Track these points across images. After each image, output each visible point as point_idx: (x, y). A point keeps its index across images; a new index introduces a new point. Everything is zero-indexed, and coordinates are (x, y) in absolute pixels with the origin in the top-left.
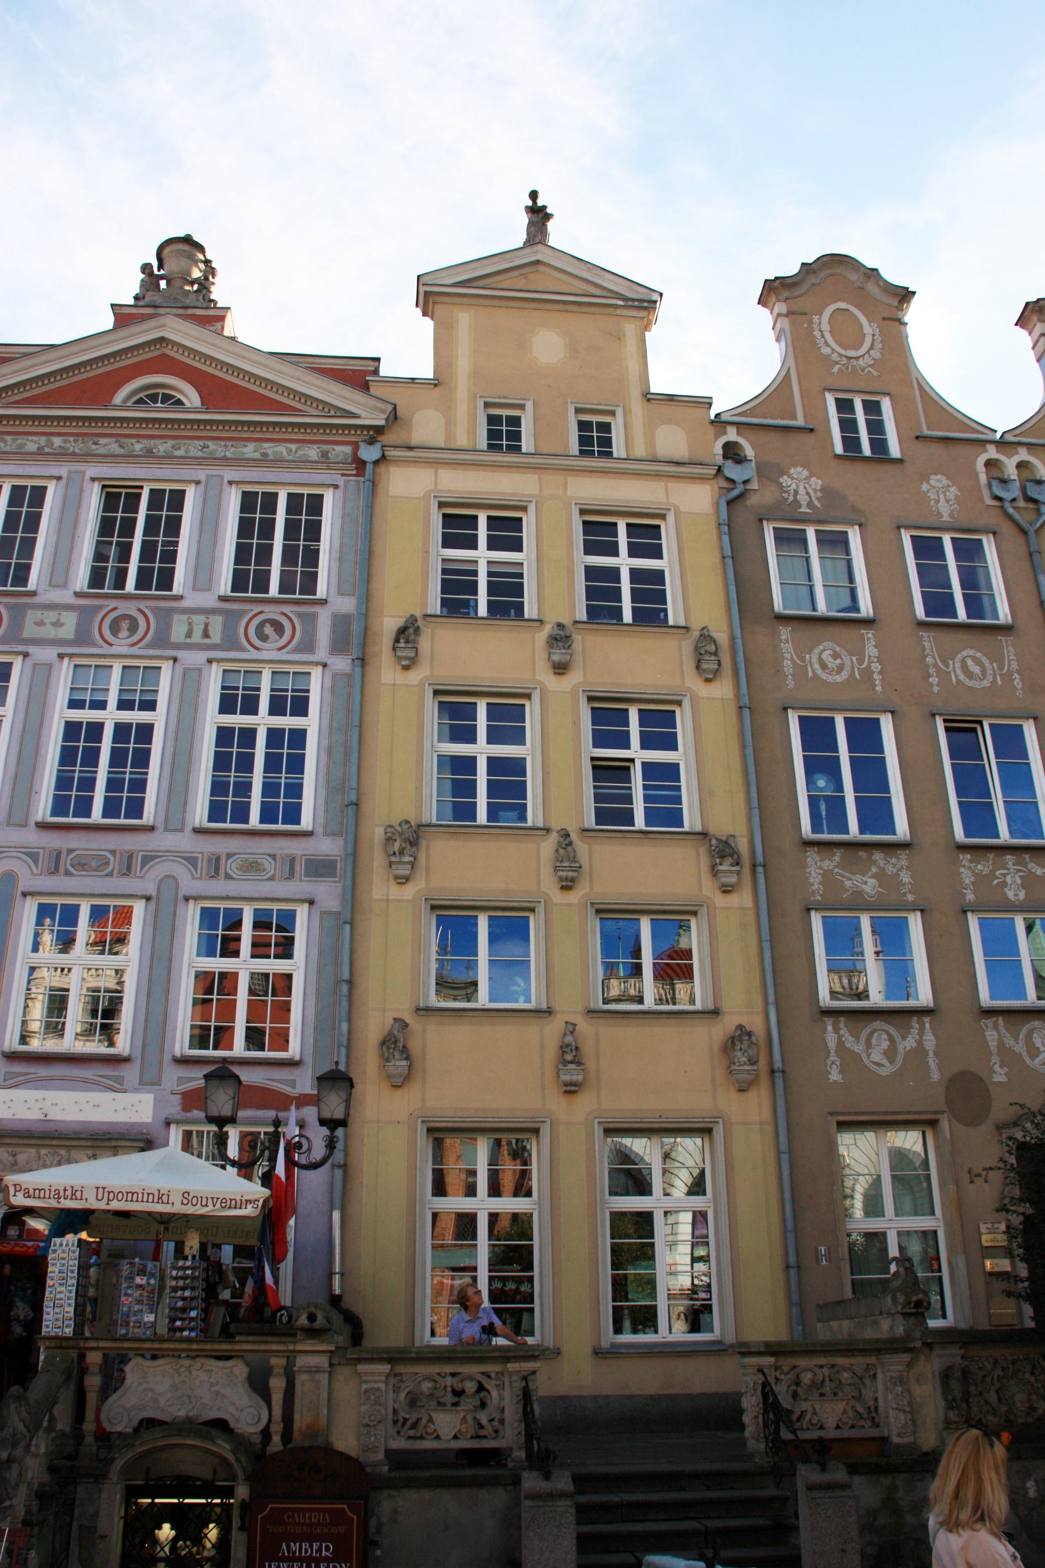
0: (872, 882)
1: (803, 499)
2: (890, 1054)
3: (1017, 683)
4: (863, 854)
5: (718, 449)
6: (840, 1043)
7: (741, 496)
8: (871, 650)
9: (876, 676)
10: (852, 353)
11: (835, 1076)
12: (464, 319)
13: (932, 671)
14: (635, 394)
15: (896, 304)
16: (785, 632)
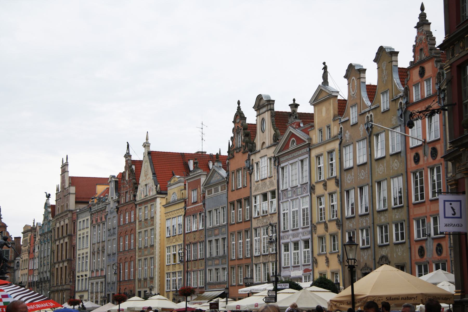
12: (316, 108)
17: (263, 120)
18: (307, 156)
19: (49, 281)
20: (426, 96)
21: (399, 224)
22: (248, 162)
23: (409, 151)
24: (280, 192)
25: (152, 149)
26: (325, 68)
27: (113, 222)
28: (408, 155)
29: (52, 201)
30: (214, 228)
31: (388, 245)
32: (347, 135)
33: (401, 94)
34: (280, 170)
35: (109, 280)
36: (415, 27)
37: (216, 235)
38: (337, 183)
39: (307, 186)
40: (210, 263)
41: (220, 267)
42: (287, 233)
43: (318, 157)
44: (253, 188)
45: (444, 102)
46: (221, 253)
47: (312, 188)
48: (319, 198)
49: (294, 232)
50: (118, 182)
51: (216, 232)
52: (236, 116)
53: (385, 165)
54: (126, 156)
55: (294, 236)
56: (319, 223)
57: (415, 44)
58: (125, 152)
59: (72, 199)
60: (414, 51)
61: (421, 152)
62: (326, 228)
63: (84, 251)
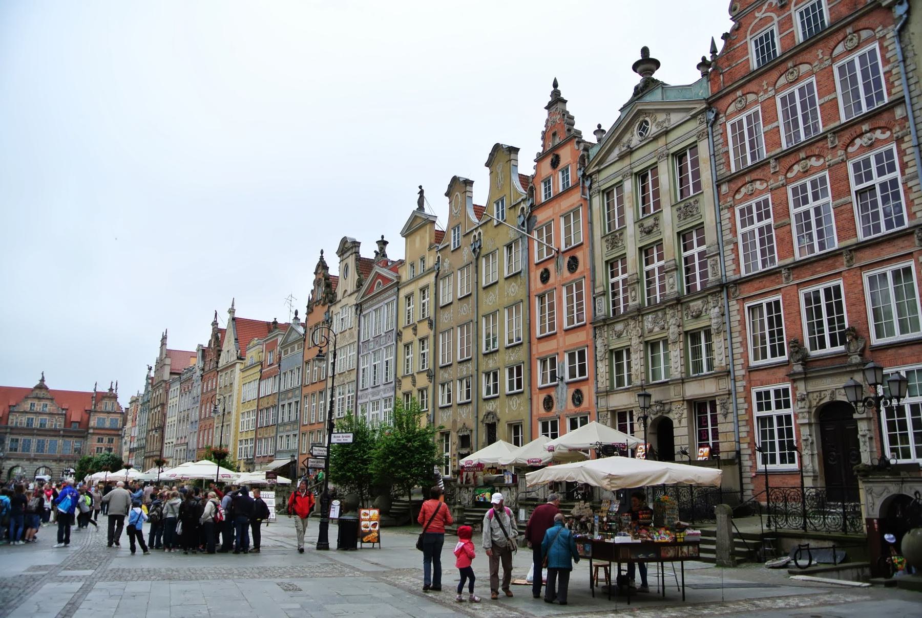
17: (347, 266)
18: (395, 297)
19: (144, 447)
20: (561, 190)
21: (516, 370)
23: (533, 267)
25: (237, 315)
26: (421, 193)
27: (197, 391)
28: (532, 274)
29: (152, 374)
30: (288, 391)
31: (498, 397)
33: (524, 196)
34: (362, 318)
35: (190, 447)
36: (546, 108)
37: (289, 399)
38: (431, 324)
40: (281, 429)
41: (291, 434)
42: (366, 392)
43: (408, 297)
46: (293, 418)
47: (399, 335)
48: (407, 346)
49: (375, 390)
50: (204, 352)
51: (290, 395)
52: (318, 266)
54: (213, 324)
55: (373, 394)
56: (404, 377)
57: (544, 129)
58: (213, 320)
59: (167, 370)
60: (543, 138)
61: (551, 267)
62: (414, 383)
63: (173, 419)
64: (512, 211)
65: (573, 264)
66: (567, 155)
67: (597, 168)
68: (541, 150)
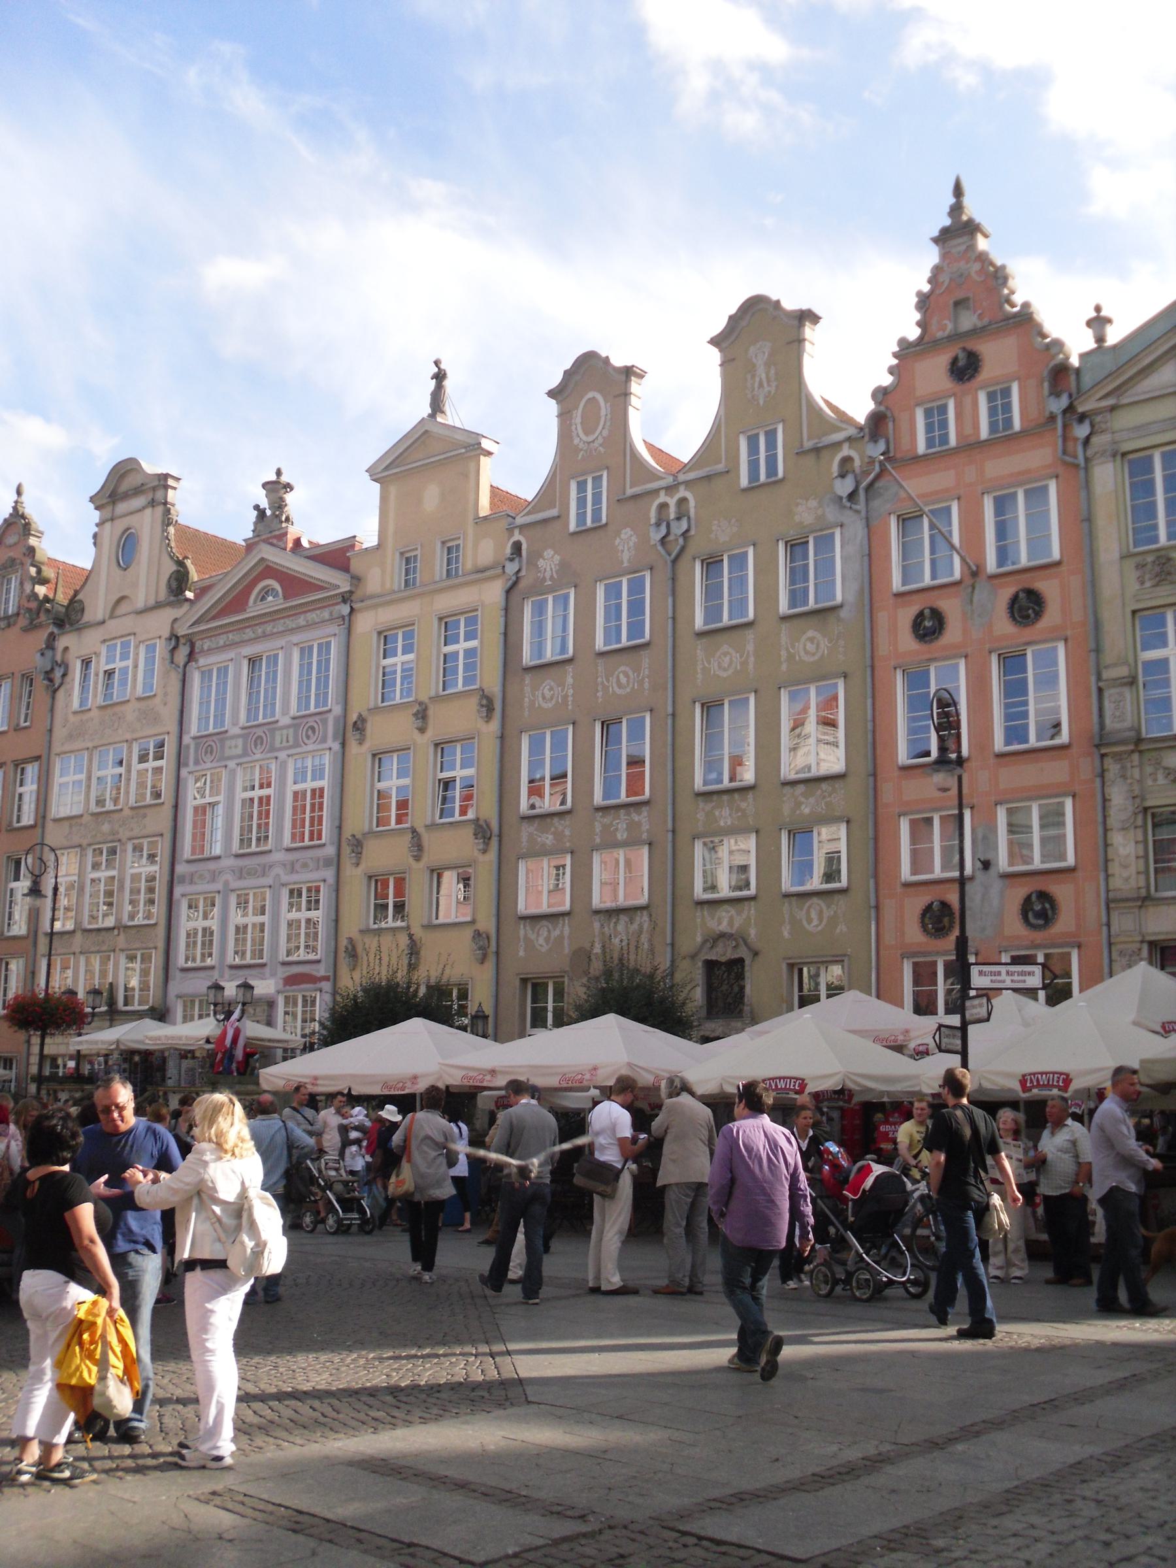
0: (551, 837)
1: (548, 575)
2: (547, 940)
3: (646, 685)
4: (548, 820)
5: (508, 550)
6: (526, 935)
7: (515, 584)
8: (570, 680)
9: (570, 699)
10: (590, 438)
11: (521, 953)
12: (393, 490)
13: (600, 688)
14: (471, 517)
15: (623, 378)
16: (528, 679)
22: (49, 653)
24: (186, 740)
26: (440, 377)
28: (882, 618)
32: (549, 562)
36: (936, 240)
38: (488, 706)
39: (325, 722)
43: (385, 637)
44: (59, 733)
45: (1085, 451)
53: (750, 647)
57: (926, 288)
61: (950, 607)
62: (418, 848)
64: (810, 460)
65: (1027, 606)
66: (998, 356)
67: (1110, 402)
68: (914, 333)
